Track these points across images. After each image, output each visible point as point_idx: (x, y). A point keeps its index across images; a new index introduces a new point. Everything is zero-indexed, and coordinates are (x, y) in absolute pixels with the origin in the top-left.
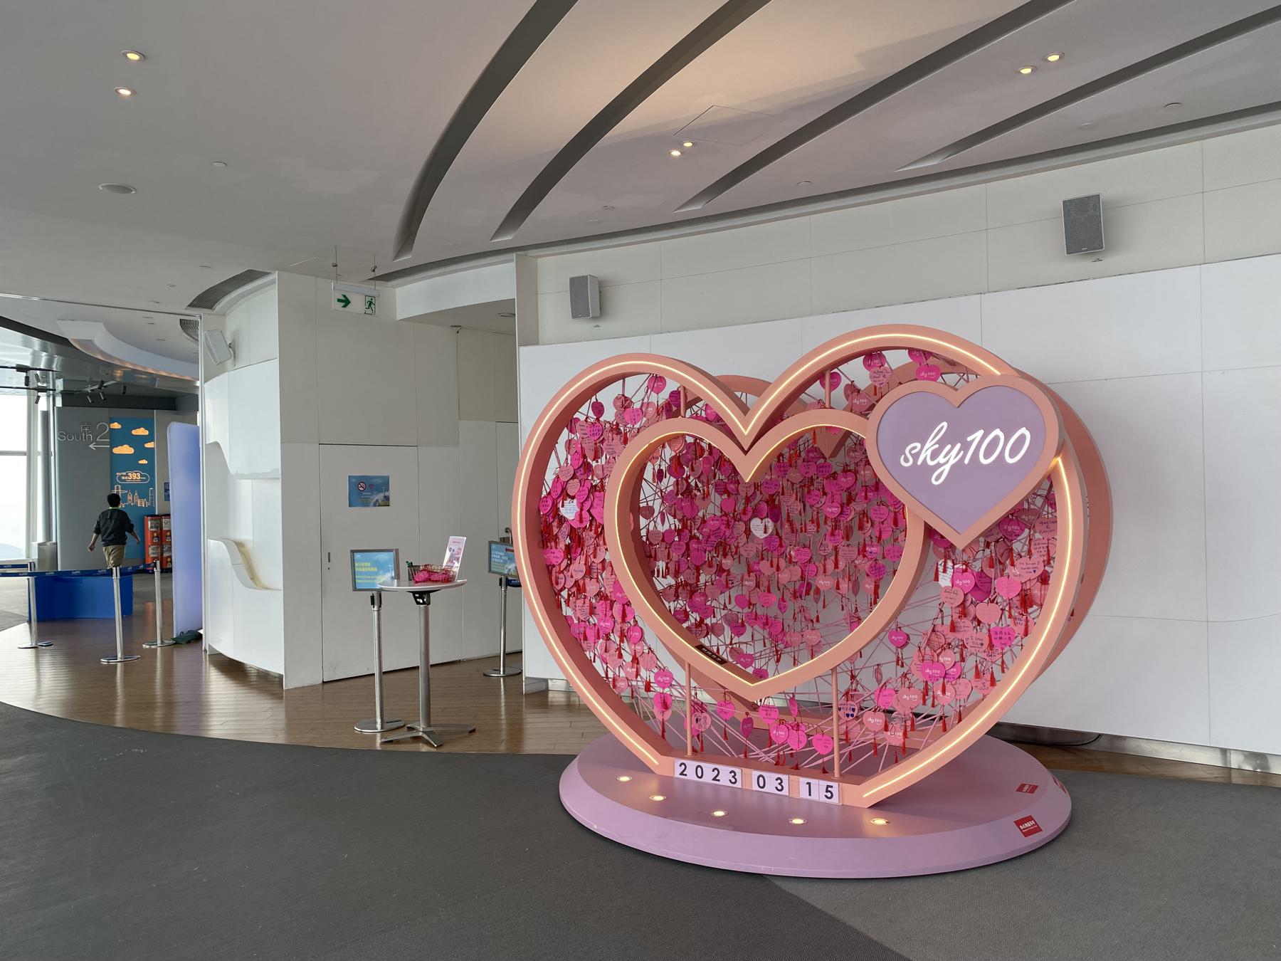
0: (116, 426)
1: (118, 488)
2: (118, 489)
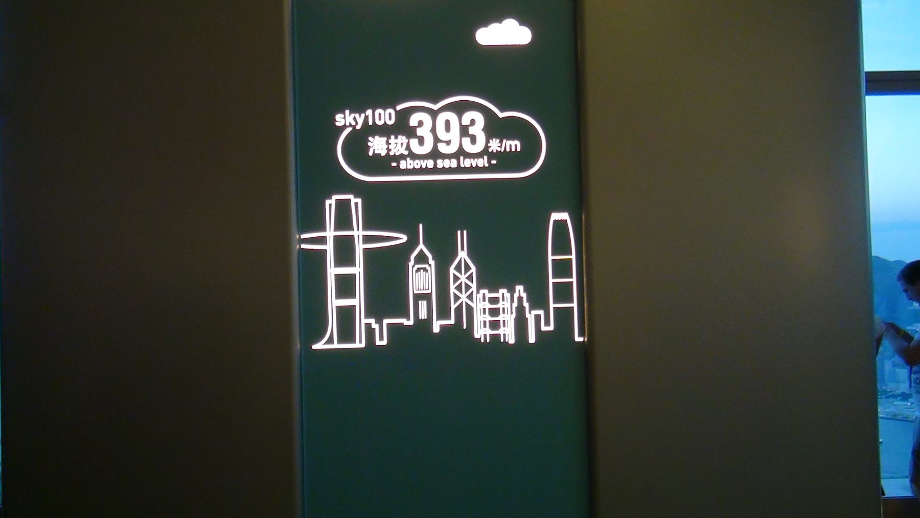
1: (343, 207)
2: (343, 220)
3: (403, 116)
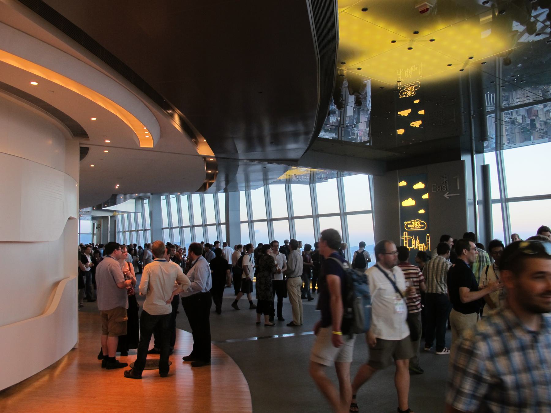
0: (403, 183)
1: (405, 234)
2: (405, 235)
3: (411, 222)
